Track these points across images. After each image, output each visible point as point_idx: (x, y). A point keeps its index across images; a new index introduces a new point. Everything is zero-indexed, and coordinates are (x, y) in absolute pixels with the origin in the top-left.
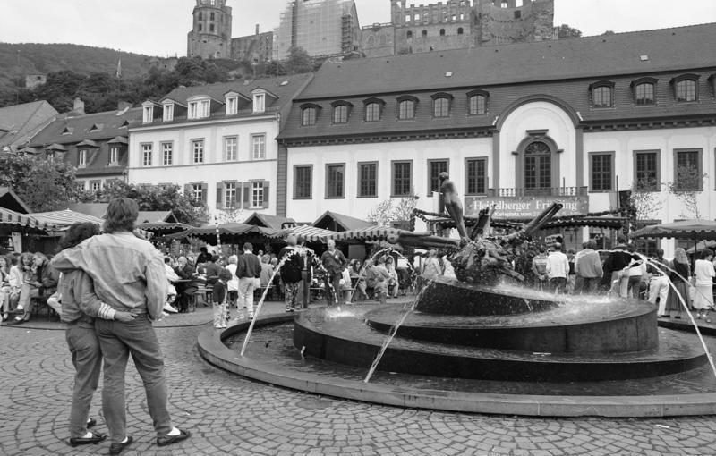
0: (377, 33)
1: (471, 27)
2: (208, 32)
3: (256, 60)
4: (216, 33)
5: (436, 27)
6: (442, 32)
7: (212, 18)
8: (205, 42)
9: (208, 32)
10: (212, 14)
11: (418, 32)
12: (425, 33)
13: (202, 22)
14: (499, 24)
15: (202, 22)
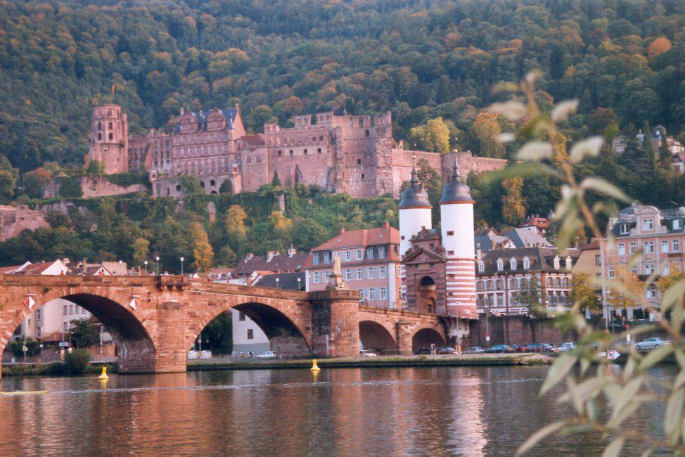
0: (254, 153)
1: (328, 147)
2: (107, 141)
3: (154, 176)
4: (114, 141)
5: (301, 148)
6: (305, 151)
7: (111, 127)
8: (105, 150)
9: (107, 141)
10: (111, 124)
11: (286, 152)
12: (291, 152)
13: (101, 132)
14: (352, 142)
15: (101, 132)
